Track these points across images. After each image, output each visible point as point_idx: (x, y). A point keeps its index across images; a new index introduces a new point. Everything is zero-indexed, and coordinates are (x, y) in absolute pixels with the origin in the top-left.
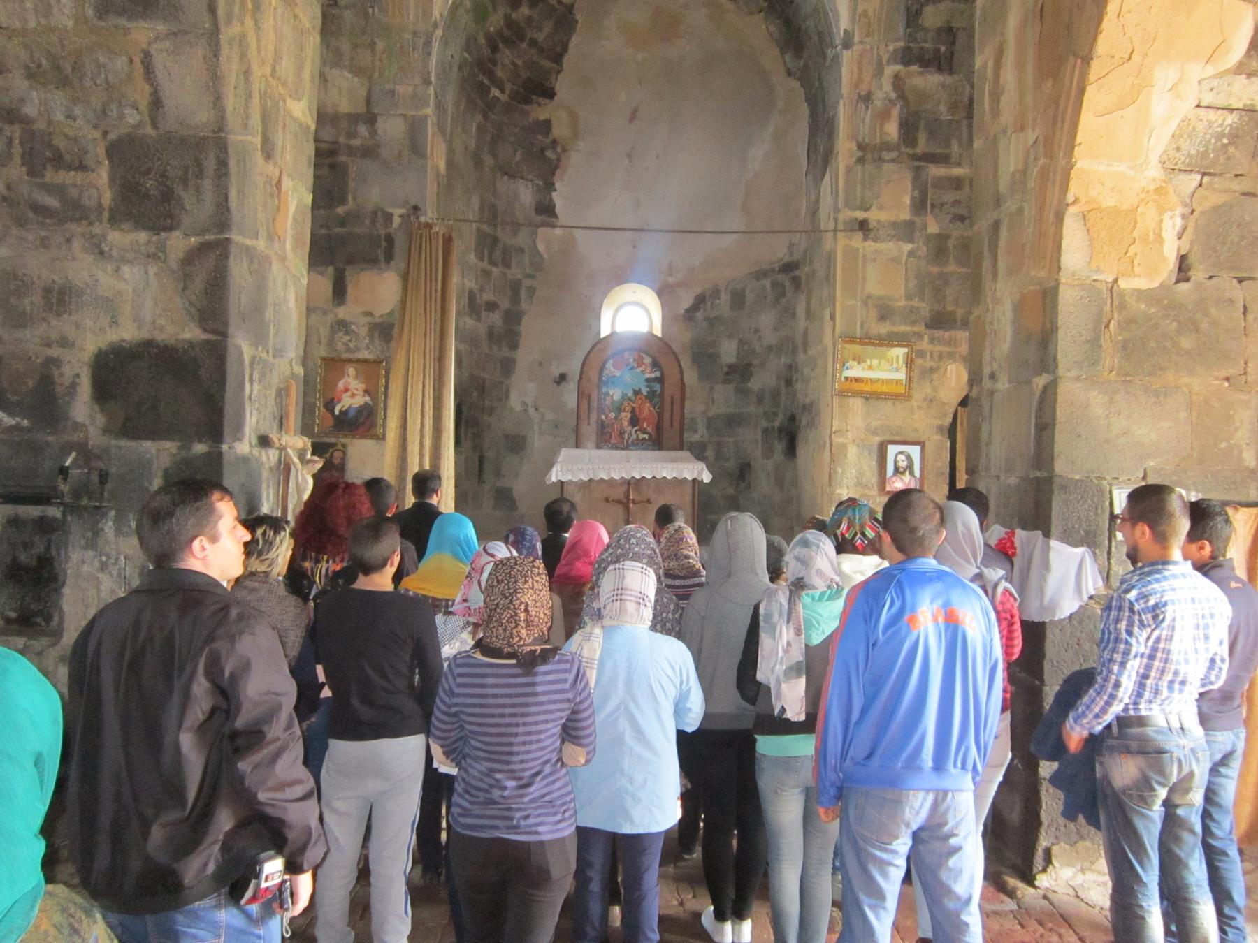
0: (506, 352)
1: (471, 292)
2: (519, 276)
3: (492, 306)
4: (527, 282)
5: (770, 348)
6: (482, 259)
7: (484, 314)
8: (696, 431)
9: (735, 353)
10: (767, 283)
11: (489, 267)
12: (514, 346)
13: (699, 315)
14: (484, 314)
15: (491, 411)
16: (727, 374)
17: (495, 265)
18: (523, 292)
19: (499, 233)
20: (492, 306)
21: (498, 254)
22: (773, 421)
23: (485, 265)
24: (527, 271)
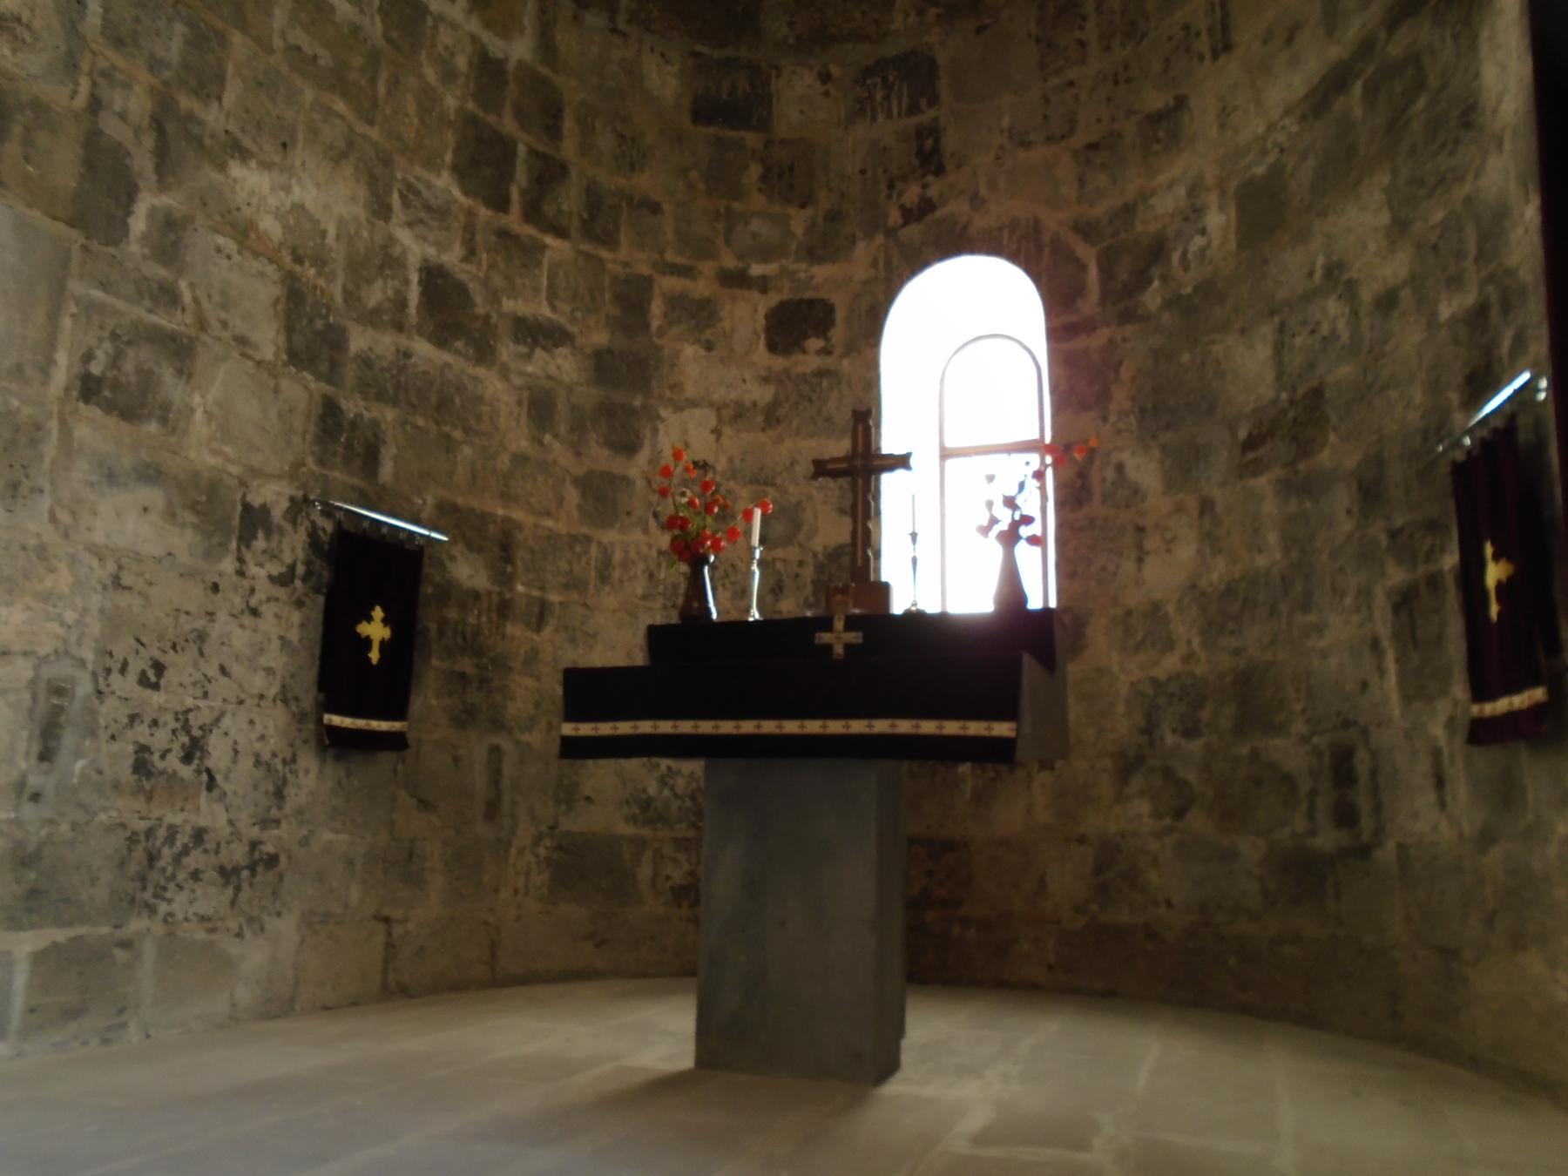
0: (600, 457)
1: (434, 276)
2: (645, 270)
3: (535, 334)
4: (670, 283)
5: (1387, 302)
6: (501, 205)
7: (507, 351)
8: (1169, 644)
9: (1269, 375)
10: (1354, 100)
11: (528, 231)
12: (628, 447)
13: (1152, 299)
14: (507, 351)
15: (540, 615)
16: (1251, 443)
17: (561, 233)
18: (656, 308)
19: (568, 149)
20: (535, 334)
21: (569, 200)
22: (1430, 556)
23: (513, 220)
24: (670, 256)
